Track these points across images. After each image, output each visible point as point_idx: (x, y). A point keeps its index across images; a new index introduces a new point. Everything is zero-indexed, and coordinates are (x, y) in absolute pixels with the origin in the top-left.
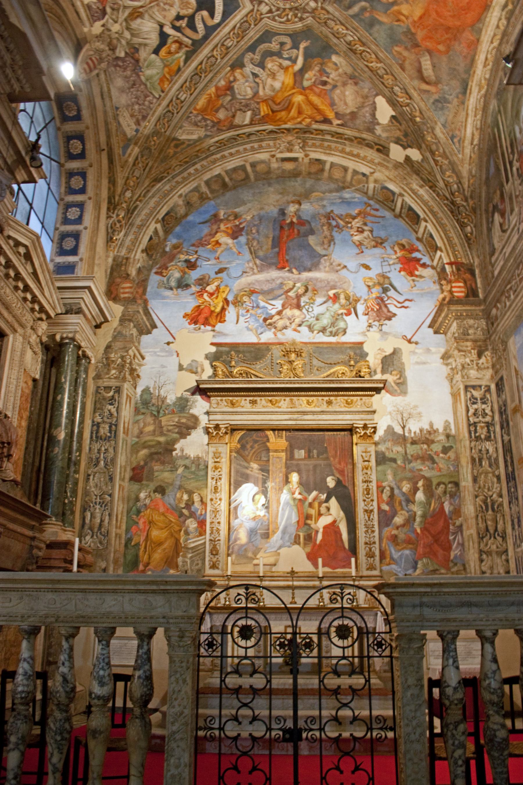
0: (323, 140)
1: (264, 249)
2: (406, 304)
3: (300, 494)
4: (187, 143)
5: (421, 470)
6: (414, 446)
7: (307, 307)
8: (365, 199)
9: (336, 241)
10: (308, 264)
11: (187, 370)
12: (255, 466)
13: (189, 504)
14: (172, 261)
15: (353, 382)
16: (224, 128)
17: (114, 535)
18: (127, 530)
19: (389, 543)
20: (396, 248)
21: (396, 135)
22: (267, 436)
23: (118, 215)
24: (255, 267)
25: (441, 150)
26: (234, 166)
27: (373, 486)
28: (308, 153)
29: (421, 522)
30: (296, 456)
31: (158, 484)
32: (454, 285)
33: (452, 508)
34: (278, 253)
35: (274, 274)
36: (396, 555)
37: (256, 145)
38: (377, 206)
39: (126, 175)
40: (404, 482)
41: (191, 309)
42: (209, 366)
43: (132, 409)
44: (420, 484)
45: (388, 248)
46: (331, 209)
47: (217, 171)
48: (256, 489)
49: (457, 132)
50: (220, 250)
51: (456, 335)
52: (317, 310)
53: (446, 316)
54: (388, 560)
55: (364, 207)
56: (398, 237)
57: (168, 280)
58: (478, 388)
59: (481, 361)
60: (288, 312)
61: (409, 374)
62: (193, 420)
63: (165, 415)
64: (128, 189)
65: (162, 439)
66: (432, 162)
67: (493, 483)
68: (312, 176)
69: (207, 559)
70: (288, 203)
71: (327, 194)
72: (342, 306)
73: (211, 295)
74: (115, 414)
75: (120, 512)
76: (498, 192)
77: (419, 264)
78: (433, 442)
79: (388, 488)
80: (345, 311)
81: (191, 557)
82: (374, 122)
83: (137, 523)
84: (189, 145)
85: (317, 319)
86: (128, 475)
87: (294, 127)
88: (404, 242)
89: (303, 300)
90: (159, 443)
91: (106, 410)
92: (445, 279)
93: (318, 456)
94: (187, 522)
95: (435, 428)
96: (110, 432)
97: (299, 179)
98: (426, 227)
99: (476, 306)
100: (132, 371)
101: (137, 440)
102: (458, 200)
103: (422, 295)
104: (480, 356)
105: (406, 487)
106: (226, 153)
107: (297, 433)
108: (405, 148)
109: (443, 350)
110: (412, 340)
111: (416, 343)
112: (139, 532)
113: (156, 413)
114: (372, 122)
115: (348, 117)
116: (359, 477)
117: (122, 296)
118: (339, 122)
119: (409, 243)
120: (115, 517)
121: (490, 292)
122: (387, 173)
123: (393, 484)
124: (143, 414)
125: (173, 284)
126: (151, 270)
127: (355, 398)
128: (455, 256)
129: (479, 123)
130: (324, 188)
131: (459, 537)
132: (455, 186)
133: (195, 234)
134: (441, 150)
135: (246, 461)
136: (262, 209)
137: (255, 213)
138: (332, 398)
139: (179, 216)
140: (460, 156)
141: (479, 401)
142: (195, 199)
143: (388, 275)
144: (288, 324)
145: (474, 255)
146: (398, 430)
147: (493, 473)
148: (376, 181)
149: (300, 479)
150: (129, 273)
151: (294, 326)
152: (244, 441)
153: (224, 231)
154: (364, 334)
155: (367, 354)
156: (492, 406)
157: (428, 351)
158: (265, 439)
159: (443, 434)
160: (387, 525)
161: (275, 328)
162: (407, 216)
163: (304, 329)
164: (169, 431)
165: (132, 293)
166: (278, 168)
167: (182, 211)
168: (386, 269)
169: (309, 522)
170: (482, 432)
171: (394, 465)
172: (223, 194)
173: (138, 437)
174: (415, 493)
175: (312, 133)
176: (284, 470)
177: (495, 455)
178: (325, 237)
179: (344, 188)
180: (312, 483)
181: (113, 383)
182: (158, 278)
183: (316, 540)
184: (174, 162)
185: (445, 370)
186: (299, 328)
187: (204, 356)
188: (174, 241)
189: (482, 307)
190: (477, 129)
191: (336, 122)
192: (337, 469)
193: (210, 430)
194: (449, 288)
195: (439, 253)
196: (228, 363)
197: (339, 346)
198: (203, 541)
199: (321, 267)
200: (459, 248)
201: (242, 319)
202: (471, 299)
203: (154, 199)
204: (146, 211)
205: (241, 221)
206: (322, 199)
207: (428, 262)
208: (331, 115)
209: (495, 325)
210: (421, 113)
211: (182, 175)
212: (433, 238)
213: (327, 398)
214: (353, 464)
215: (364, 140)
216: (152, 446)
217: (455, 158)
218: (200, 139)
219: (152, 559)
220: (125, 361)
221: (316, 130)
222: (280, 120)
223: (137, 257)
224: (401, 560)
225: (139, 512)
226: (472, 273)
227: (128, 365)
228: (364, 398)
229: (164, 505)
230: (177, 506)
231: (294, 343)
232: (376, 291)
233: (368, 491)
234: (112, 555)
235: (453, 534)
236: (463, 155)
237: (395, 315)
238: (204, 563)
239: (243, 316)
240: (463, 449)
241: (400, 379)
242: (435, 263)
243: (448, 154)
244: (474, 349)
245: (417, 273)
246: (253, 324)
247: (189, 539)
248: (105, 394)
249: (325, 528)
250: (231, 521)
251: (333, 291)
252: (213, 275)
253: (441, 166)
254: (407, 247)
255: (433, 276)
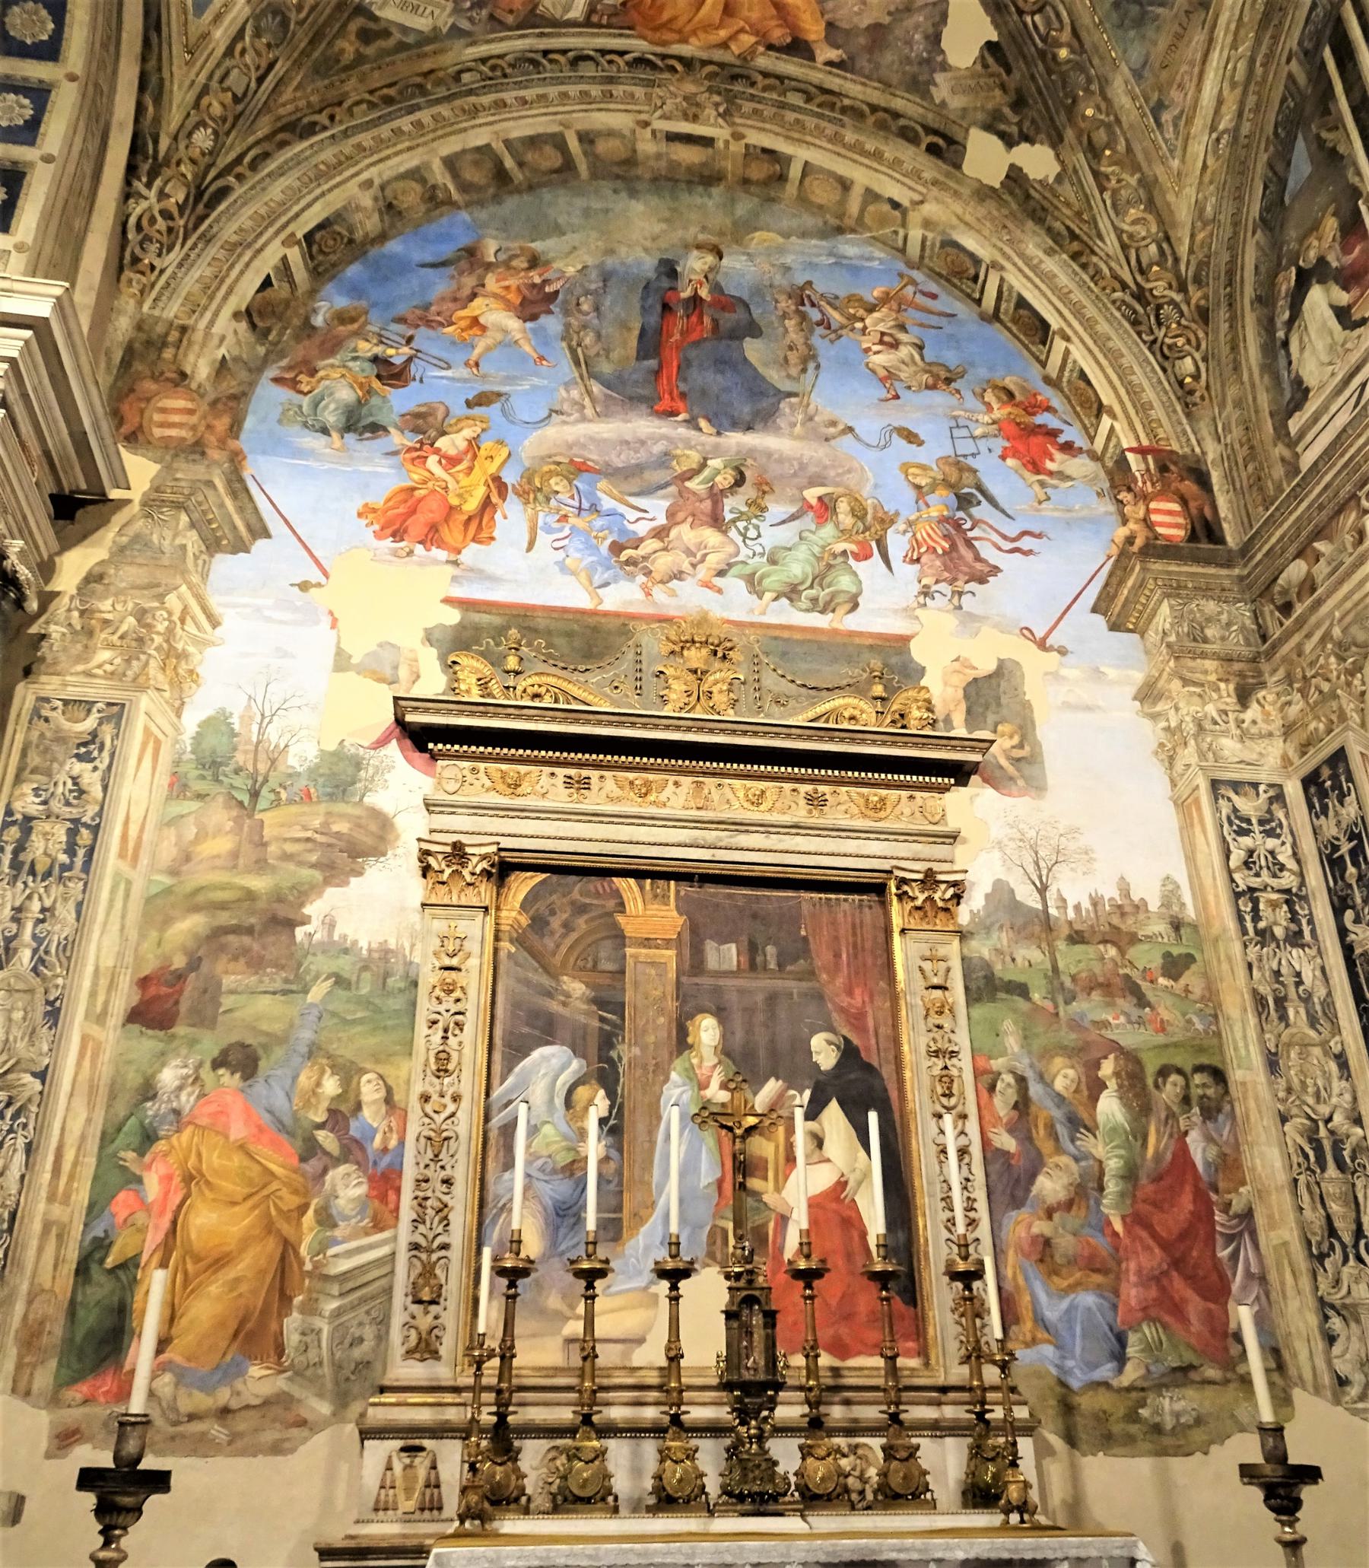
0: (783, 106)
1: (615, 355)
2: (1026, 543)
3: (724, 1086)
4: (397, 36)
5: (1106, 1024)
6: (1079, 948)
7: (741, 525)
8: (901, 266)
9: (822, 360)
10: (745, 411)
11: (361, 670)
12: (576, 988)
13: (338, 1117)
14: (332, 352)
15: (893, 738)
16: (510, 19)
17: (37, 1226)
18: (94, 1209)
19: (1027, 1264)
20: (989, 397)
21: (990, 106)
22: (617, 894)
23: (162, 195)
24: (587, 401)
25: (1121, 147)
26: (529, 132)
27: (964, 1065)
28: (741, 130)
29: (1122, 1195)
30: (712, 961)
31: (234, 1038)
32: (1153, 505)
33: (1212, 1152)
34: (657, 373)
35: (643, 426)
36: (1053, 1311)
37: (595, 90)
38: (933, 287)
39: (202, 78)
40: (1059, 1061)
41: (387, 494)
42: (437, 665)
43: (163, 780)
44: (1107, 1068)
45: (967, 395)
46: (807, 278)
47: (479, 137)
48: (576, 1065)
49: (1175, 94)
50: (481, 345)
51: (1172, 638)
52: (772, 536)
53: (1141, 585)
54: (1028, 1325)
55: (897, 285)
56: (991, 369)
57: (316, 405)
58: (1252, 791)
59: (1248, 715)
60: (685, 533)
61: (1048, 732)
62: (373, 827)
63: (277, 803)
64: (205, 126)
65: (259, 883)
66: (1089, 180)
67: (1328, 1079)
68: (752, 189)
69: (398, 1319)
70: (687, 247)
71: (793, 239)
72: (844, 533)
73: (451, 462)
74: (97, 791)
75: (71, 1140)
76: (1331, 225)
77: (1055, 444)
78: (1134, 939)
79: (1009, 1078)
80: (854, 547)
81: (338, 1313)
82: (933, 57)
83: (139, 1180)
84: (402, 47)
85: (773, 561)
86: (123, 999)
87: (704, 56)
88: (1009, 382)
89: (731, 505)
90: (250, 895)
91: (62, 777)
92: (1129, 490)
93: (781, 965)
94: (328, 1178)
95: (1136, 897)
96: (71, 851)
97: (716, 191)
98: (1067, 352)
99: (1222, 566)
100: (172, 655)
101: (167, 880)
102: (1159, 289)
103: (1068, 523)
104: (1244, 696)
105: (1065, 1077)
106: (509, 96)
107: (711, 889)
108: (1009, 142)
109: (1138, 677)
110: (1049, 642)
111: (1062, 652)
112: (140, 1218)
113: (245, 798)
114: (928, 61)
115: (862, 41)
116: (914, 1042)
117: (158, 432)
118: (833, 54)
119: (1023, 389)
120: (51, 1158)
121: (1271, 522)
122: (957, 207)
123: (1023, 1066)
124: (200, 796)
125: (331, 416)
126: (260, 370)
127: (893, 794)
128: (1152, 433)
129: (1242, 66)
130: (785, 224)
131: (1247, 1251)
132: (1153, 248)
133: (406, 293)
134: (1121, 147)
135: (546, 969)
136: (611, 252)
137: (590, 261)
138: (822, 788)
139: (359, 235)
140: (1175, 164)
141: (1256, 828)
142: (411, 197)
143: (970, 462)
144: (686, 566)
145: (1205, 430)
146: (1028, 897)
147: (1324, 1045)
148: (927, 224)
149: (724, 1036)
150: (188, 371)
151: (702, 572)
152: (541, 906)
153: (495, 296)
154: (908, 612)
155: (922, 671)
156: (1294, 845)
157: (1097, 674)
158: (611, 904)
159: (1161, 916)
160: (1017, 1202)
161: (648, 573)
162: (1015, 321)
163: (734, 585)
164: (287, 857)
165: (194, 428)
166: (659, 156)
167: (369, 224)
168: (965, 447)
169: (754, 1183)
170: (1278, 920)
171: (1020, 1003)
172: (497, 199)
173: (174, 872)
174: (1094, 1099)
175: (753, 84)
176: (672, 1005)
177: (1321, 992)
178: (791, 348)
179: (840, 230)
180: (762, 1053)
181: (99, 691)
182: (284, 394)
183: (781, 1250)
184: (353, 88)
185: (1150, 733)
186: (718, 582)
187: (421, 634)
188: (342, 302)
189: (1237, 571)
190: (1233, 85)
191: (826, 53)
192: (842, 1010)
193: (431, 860)
194: (1141, 514)
195: (1106, 422)
196: (496, 661)
197: (839, 639)
198: (385, 1250)
199: (781, 422)
200: (1158, 412)
201: (543, 539)
202: (1205, 546)
203: (283, 183)
204: (257, 207)
205: (546, 276)
206: (781, 250)
207: (1081, 442)
208: (813, 30)
209: (1299, 609)
210: (1075, 32)
211: (375, 132)
212: (1089, 383)
213: (808, 788)
214: (894, 998)
215: (896, 115)
216: (223, 906)
217: (1159, 171)
218: (434, 37)
219: (183, 1323)
220: (149, 627)
221: (766, 75)
222: (666, 26)
223: (217, 329)
224: (1071, 1329)
225: (148, 1138)
226: (1202, 479)
227: (158, 640)
228: (918, 794)
229: (247, 1110)
230: (296, 1118)
231: (703, 620)
232: (939, 503)
233: (947, 1084)
234: (19, 1308)
235: (1230, 1239)
236: (1183, 161)
237: (995, 570)
238: (382, 1338)
239: (549, 530)
240: (1225, 966)
241: (1021, 746)
242: (1099, 444)
243: (1140, 157)
244: (1227, 681)
245: (1050, 465)
246: (577, 556)
247: (335, 1242)
248: (66, 725)
249: (815, 1205)
250: (490, 1177)
251: (820, 491)
252: (459, 409)
253: (1115, 193)
254: (1019, 397)
255: (1096, 477)
